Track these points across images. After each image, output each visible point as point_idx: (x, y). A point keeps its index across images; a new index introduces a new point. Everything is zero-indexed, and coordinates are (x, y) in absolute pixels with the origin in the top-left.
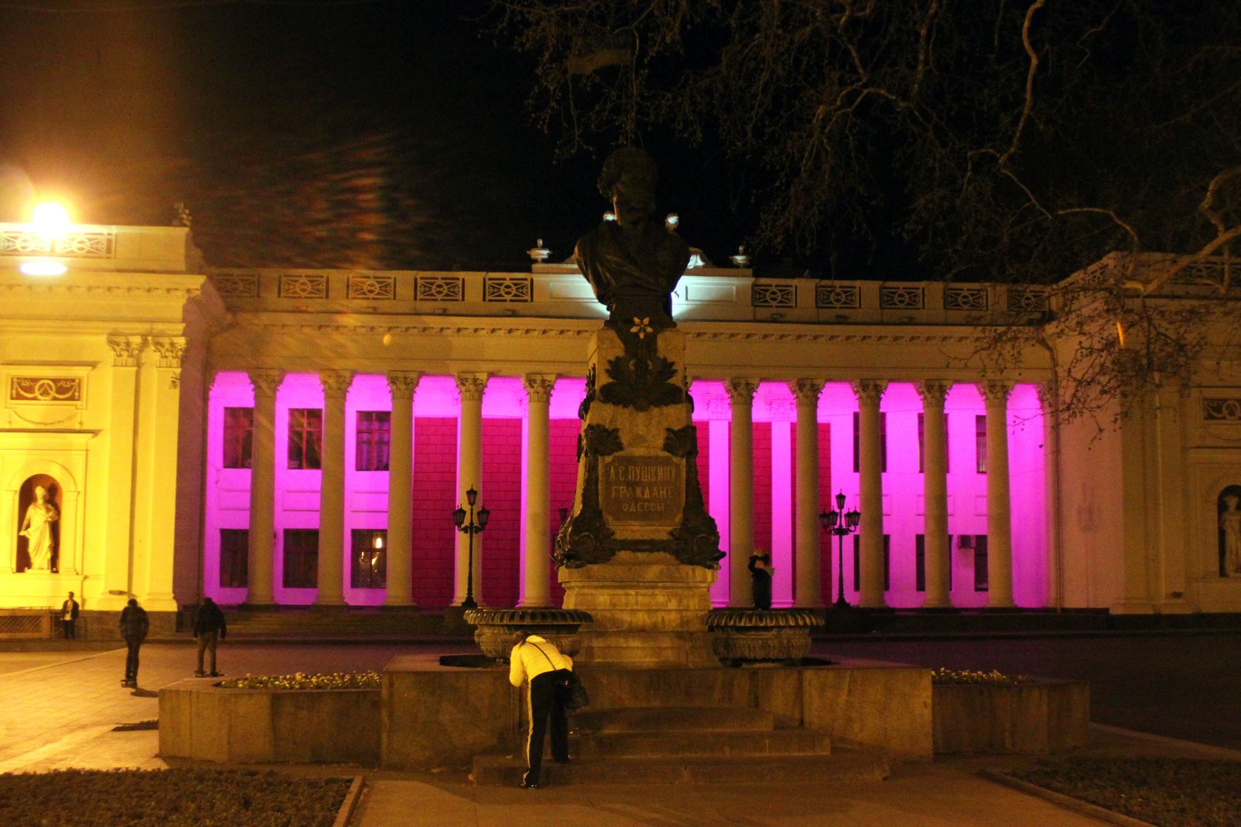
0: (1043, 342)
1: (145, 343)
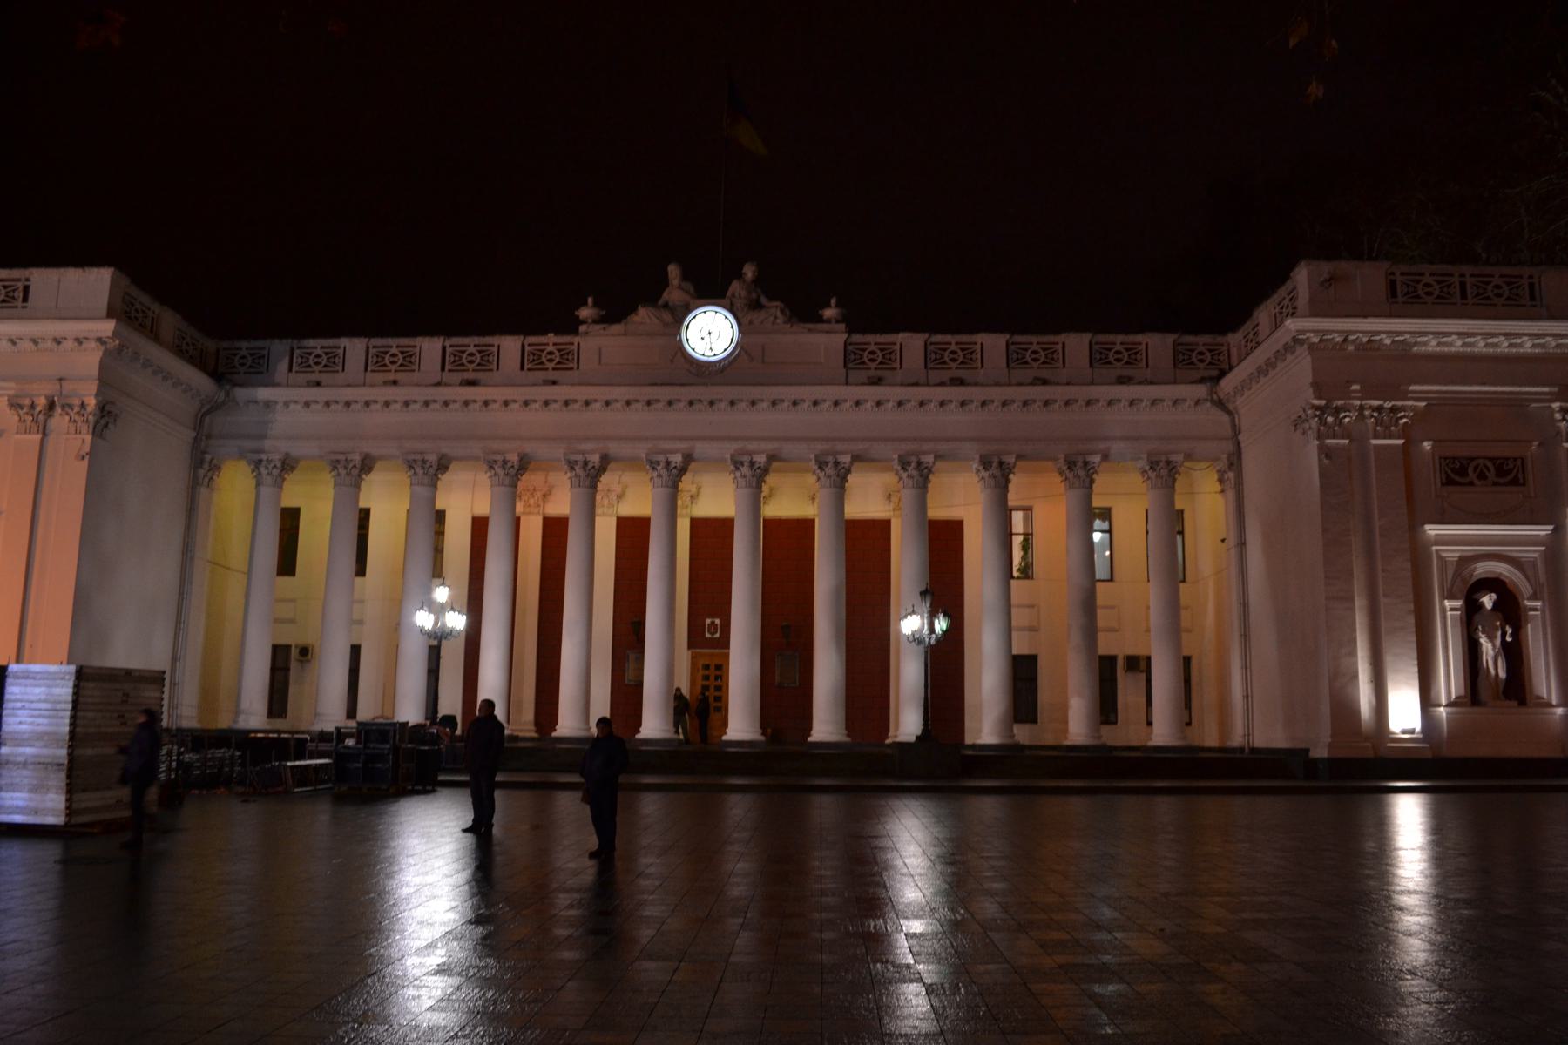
0: (1220, 404)
1: (51, 406)
